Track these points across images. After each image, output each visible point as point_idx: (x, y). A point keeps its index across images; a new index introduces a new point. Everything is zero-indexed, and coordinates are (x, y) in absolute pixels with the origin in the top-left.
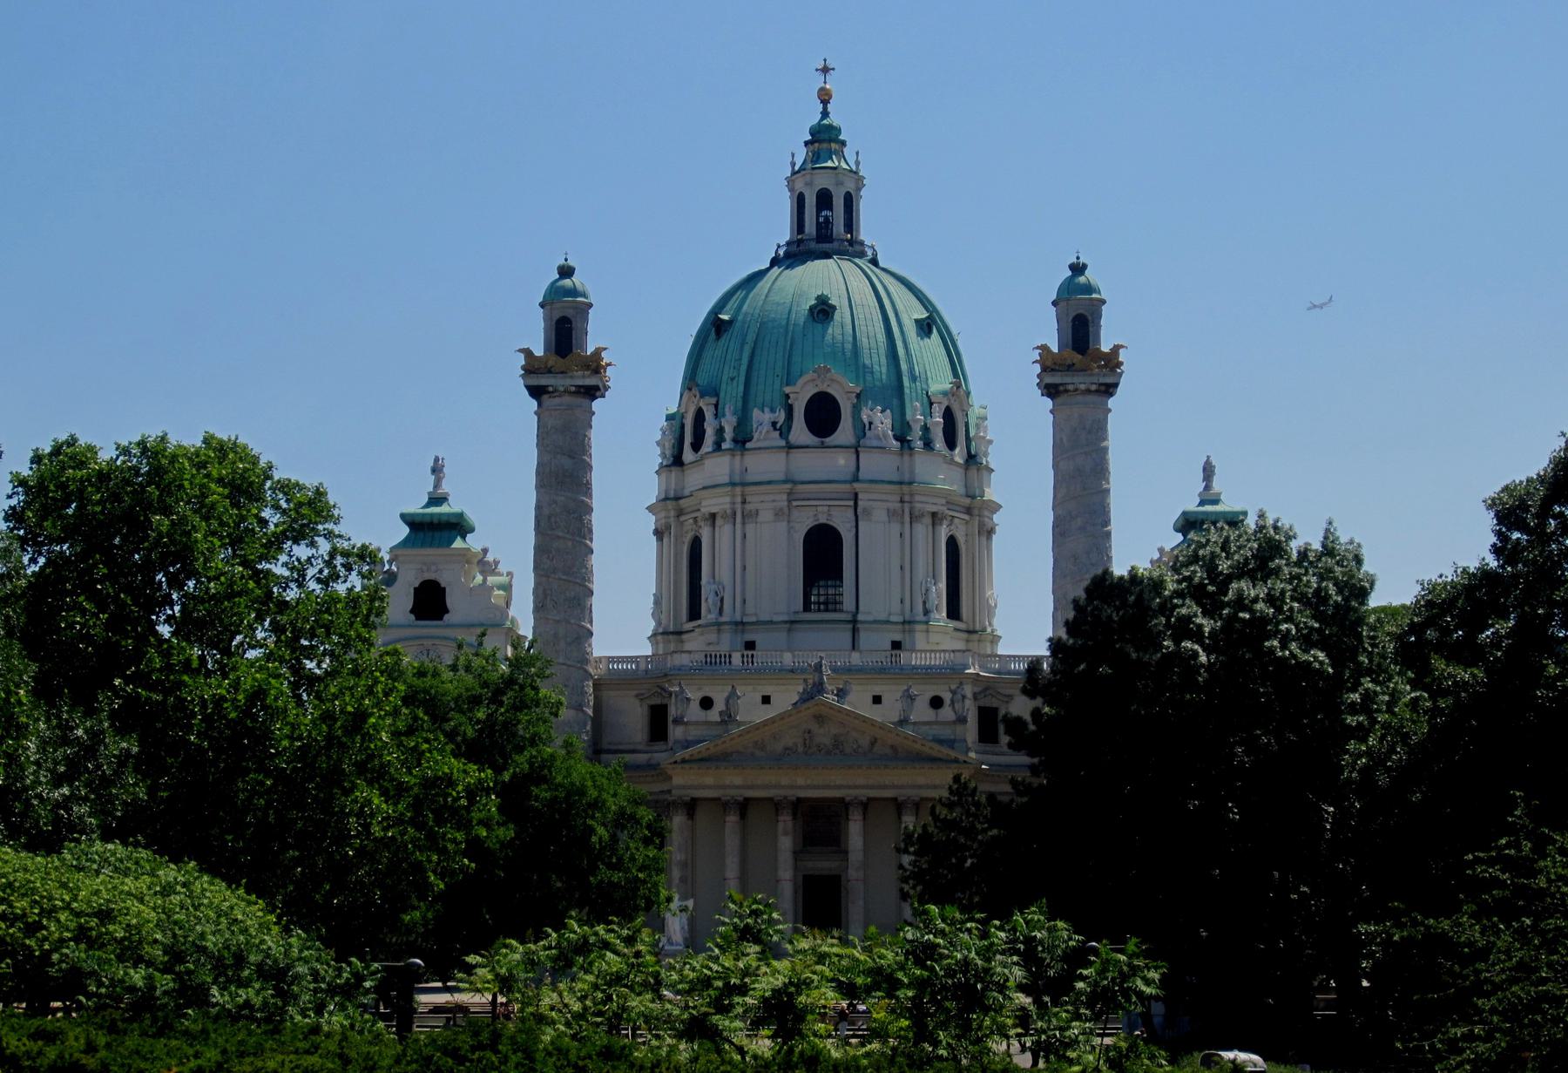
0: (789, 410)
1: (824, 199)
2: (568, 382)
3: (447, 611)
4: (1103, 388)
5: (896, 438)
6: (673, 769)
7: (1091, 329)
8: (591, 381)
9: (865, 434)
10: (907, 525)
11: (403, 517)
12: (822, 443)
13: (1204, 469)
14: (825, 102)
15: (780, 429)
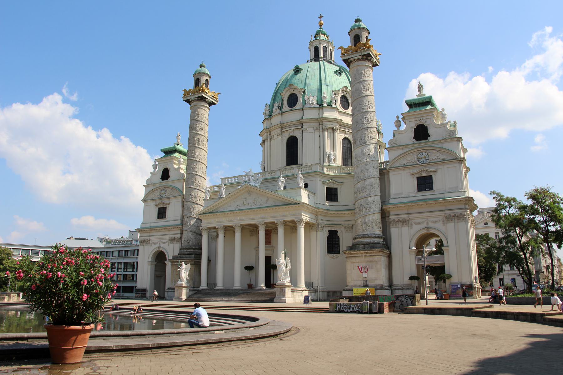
0: (283, 100)
1: (316, 49)
2: (194, 96)
3: (169, 177)
4: (365, 57)
5: (318, 104)
6: (201, 216)
7: (360, 39)
8: (200, 95)
9: (306, 104)
10: (321, 133)
11: (161, 150)
12: (292, 109)
13: (419, 87)
14: (320, 26)
15: (280, 107)
